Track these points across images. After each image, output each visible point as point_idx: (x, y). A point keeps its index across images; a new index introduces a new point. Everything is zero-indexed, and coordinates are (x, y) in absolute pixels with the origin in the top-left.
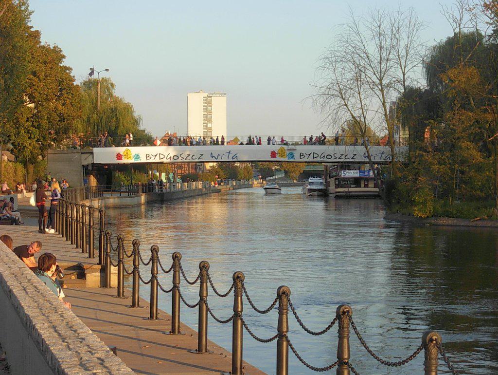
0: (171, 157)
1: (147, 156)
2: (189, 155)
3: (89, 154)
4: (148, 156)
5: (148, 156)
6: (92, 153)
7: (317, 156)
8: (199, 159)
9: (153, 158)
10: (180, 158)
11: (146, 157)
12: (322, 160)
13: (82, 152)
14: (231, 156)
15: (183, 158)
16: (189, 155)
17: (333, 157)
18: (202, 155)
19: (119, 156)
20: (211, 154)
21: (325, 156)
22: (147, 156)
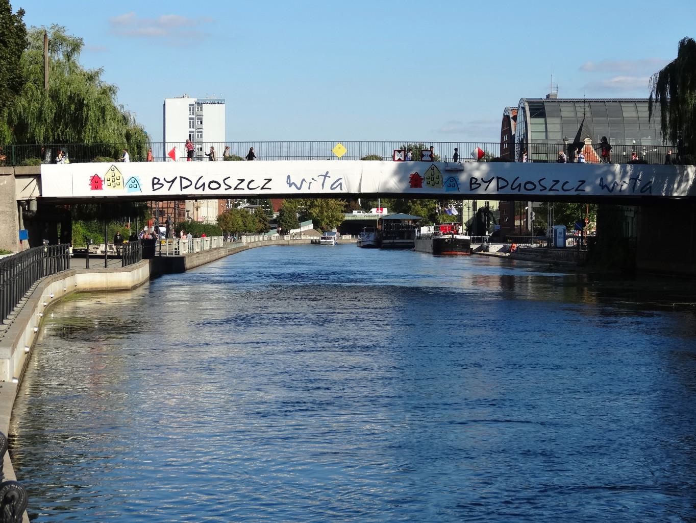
0: (204, 184)
1: (155, 182)
2: (243, 180)
3: (28, 180)
4: (156, 181)
5: (156, 181)
6: (38, 177)
7: (505, 184)
8: (262, 188)
9: (167, 185)
10: (223, 186)
11: (153, 184)
12: (516, 192)
13: (16, 173)
14: (329, 182)
15: (230, 187)
16: (243, 180)
17: (539, 187)
18: (270, 180)
19: (96, 182)
20: (289, 177)
21: (522, 186)
22: (155, 182)
